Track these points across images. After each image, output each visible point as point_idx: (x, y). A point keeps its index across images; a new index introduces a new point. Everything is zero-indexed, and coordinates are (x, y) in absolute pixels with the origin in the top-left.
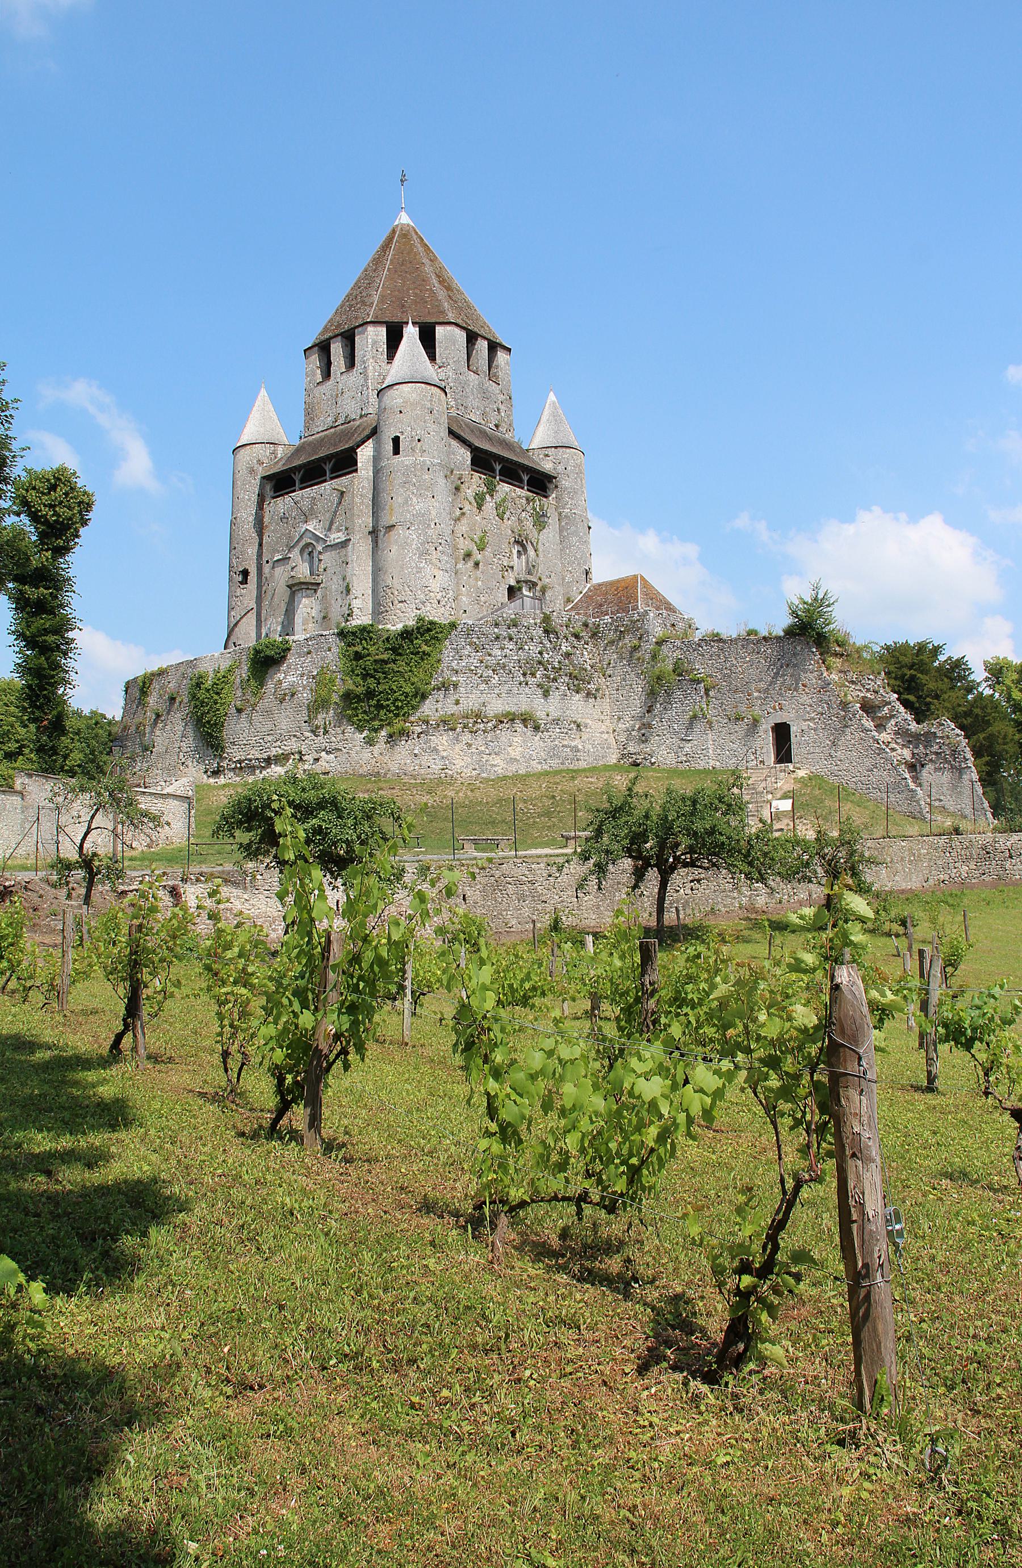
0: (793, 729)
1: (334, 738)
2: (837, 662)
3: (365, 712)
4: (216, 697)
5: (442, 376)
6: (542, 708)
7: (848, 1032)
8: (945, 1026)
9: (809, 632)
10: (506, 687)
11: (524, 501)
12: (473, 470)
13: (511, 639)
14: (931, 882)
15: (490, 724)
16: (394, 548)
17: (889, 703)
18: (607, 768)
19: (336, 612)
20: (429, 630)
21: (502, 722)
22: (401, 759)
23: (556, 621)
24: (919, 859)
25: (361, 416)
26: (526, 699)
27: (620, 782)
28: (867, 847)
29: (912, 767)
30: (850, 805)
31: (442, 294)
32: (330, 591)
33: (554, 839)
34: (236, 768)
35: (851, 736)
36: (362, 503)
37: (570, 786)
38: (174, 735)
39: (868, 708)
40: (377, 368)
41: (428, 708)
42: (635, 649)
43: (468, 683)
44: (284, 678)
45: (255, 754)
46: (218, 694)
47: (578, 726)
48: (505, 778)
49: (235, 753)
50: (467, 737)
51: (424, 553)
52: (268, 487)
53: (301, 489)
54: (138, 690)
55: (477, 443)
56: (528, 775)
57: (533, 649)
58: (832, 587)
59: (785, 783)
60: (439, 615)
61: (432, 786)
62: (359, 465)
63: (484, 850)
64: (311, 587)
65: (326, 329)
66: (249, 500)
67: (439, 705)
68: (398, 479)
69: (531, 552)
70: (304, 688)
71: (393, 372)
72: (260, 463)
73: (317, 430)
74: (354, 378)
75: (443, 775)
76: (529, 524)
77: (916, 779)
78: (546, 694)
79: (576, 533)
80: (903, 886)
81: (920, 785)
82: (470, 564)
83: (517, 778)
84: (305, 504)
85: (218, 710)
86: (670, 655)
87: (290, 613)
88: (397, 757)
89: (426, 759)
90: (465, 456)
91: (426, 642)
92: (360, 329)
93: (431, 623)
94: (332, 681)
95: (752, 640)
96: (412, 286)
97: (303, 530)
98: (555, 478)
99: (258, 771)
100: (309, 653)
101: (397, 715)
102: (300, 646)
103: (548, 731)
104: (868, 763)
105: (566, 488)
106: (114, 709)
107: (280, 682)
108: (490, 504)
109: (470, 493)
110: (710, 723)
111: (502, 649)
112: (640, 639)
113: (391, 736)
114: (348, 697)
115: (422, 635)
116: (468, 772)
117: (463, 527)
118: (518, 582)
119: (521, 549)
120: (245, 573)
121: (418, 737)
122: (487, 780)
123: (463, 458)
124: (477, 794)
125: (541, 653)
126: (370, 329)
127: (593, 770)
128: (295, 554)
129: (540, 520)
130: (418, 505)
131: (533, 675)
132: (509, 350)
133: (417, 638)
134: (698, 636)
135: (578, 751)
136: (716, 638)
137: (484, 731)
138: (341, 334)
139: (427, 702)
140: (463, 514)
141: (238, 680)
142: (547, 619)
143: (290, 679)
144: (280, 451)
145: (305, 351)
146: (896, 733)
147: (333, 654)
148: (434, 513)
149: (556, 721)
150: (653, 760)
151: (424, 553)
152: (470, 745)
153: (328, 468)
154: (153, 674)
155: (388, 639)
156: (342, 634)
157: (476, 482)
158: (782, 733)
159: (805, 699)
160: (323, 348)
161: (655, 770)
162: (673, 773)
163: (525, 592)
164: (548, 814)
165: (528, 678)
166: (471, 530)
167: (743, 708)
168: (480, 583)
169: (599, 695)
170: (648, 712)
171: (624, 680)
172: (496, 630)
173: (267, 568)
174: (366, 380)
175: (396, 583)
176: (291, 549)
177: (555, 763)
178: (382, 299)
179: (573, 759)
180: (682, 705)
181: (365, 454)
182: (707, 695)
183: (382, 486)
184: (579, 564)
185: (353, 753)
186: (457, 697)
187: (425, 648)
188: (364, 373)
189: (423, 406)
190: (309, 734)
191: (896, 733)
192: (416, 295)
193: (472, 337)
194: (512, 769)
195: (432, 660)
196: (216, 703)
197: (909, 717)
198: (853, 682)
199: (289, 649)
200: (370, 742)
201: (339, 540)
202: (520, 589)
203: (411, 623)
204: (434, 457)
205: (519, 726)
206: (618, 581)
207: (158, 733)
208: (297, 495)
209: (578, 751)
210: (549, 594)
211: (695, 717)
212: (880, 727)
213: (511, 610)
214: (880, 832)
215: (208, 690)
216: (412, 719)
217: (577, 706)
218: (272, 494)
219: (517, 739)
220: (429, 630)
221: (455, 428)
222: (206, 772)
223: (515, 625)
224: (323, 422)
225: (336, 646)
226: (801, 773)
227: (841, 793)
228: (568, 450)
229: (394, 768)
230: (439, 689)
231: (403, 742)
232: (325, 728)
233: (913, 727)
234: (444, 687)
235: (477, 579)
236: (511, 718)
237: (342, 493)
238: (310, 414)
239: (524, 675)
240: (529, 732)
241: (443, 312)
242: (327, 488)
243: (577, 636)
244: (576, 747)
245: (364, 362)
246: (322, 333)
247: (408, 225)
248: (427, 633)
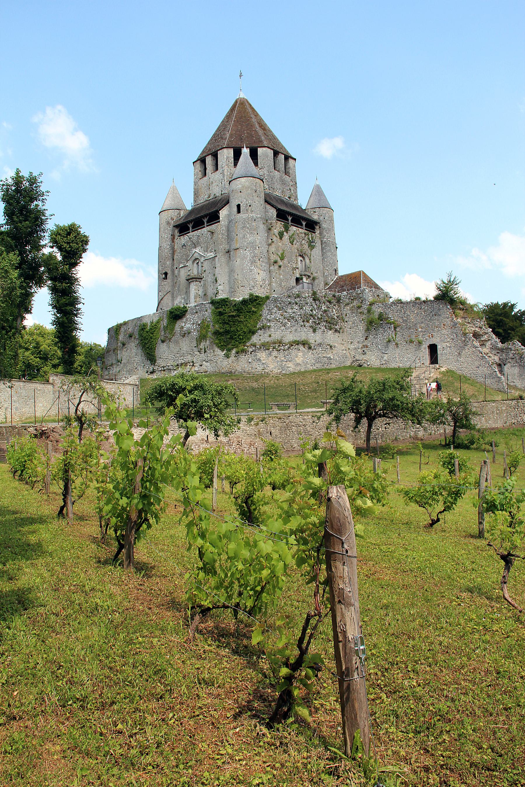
0: (439, 347)
1: (210, 355)
2: (461, 313)
3: (224, 341)
4: (151, 335)
5: (261, 173)
6: (314, 338)
7: (335, 527)
8: (487, 503)
9: (446, 297)
10: (294, 328)
11: (303, 235)
12: (277, 220)
13: (297, 304)
14: (508, 424)
15: (286, 347)
16: (238, 260)
17: (487, 333)
18: (345, 367)
19: (211, 292)
20: (256, 300)
21: (292, 345)
22: (242, 364)
23: (319, 295)
24: (501, 412)
25: (222, 194)
26: (305, 333)
27: (351, 374)
28: (474, 406)
29: (499, 365)
30: (467, 385)
31: (261, 132)
32: (208, 282)
33: (318, 403)
34: (162, 370)
35: (468, 351)
36: (222, 238)
37: (326, 377)
38: (132, 353)
39: (476, 335)
40: (229, 170)
41: (255, 339)
42: (359, 307)
43: (275, 327)
44: (185, 325)
45: (170, 363)
46: (152, 334)
48: (294, 373)
49: (160, 362)
50: (275, 353)
51: (253, 262)
52: (176, 231)
53: (192, 231)
54: (114, 332)
55: (280, 207)
56: (306, 372)
57: (307, 309)
58: (458, 275)
59: (434, 375)
60: (260, 293)
61: (257, 377)
62: (221, 219)
63: (282, 410)
64: (198, 279)
65: (203, 152)
66: (167, 238)
67: (261, 338)
68: (240, 226)
69: (307, 261)
70: (194, 330)
71: (237, 171)
72: (172, 219)
73: (200, 202)
74: (217, 176)
75: (263, 372)
76: (306, 246)
77: (501, 372)
78: (314, 331)
79: (330, 251)
80: (494, 426)
81: (504, 375)
82: (276, 267)
83: (300, 373)
84: (195, 239)
85: (153, 342)
86: (377, 310)
87: (187, 293)
88: (240, 363)
89: (255, 365)
90: (273, 212)
91: (254, 306)
92: (220, 151)
93: (257, 297)
94: (208, 326)
95: (417, 302)
96: (246, 129)
97: (193, 252)
98: (319, 223)
99: (172, 372)
100: (197, 313)
101: (240, 343)
102: (192, 309)
103: (315, 350)
104: (477, 363)
105: (325, 228)
106: (102, 341)
107: (182, 327)
108: (286, 236)
109: (276, 232)
110: (397, 344)
112: (361, 303)
113: (237, 353)
114: (216, 333)
115: (252, 302)
116: (276, 371)
117: (273, 249)
118: (301, 275)
119: (302, 259)
120: (166, 274)
121: (251, 354)
122: (285, 374)
123: (272, 214)
124: (280, 381)
125: (311, 311)
126: (225, 150)
127: (338, 369)
128: (190, 263)
129: (311, 246)
131: (308, 321)
132: (295, 159)
133: (249, 304)
134: (391, 300)
135: (331, 359)
136: (399, 302)
137: (284, 350)
138: (211, 154)
139: (255, 336)
140: (273, 242)
141: (162, 327)
142: (314, 293)
143: (187, 326)
144: (182, 213)
145: (193, 163)
146: (491, 348)
147: (208, 313)
148: (258, 242)
149: (320, 345)
150: (368, 364)
151: (253, 262)
152: (277, 357)
153: (205, 221)
154: (121, 325)
155: (235, 305)
156: (213, 303)
157: (279, 226)
158: (433, 348)
159: (444, 331)
160: (202, 160)
161: (369, 368)
162: (379, 370)
163: (304, 280)
164: (315, 391)
165: (305, 323)
166: (277, 250)
167: (413, 337)
168: (281, 276)
169: (341, 331)
170: (366, 339)
171: (354, 323)
173: (176, 272)
174: (224, 176)
175: (240, 277)
176: (187, 261)
177: (319, 366)
178: (231, 136)
179: (328, 364)
180: (382, 335)
181: (223, 213)
182: (395, 330)
183: (231, 229)
184: (331, 266)
185: (219, 362)
186: (269, 333)
187: (253, 309)
188: (223, 173)
189: (252, 189)
190: (196, 353)
191: (491, 348)
192: (248, 133)
193: (276, 153)
194: (298, 368)
195: (258, 315)
196: (151, 338)
197: (498, 340)
198: (469, 323)
199: (187, 311)
200: (227, 356)
201: (211, 257)
202: (302, 279)
203: (247, 297)
204: (258, 214)
205: (301, 347)
206: (351, 274)
207: (124, 353)
208: (191, 234)
209: (331, 359)
210: (317, 281)
211: (389, 341)
212: (483, 345)
213: (296, 291)
214: (481, 398)
215: (147, 332)
216: (248, 344)
217: (330, 337)
218: (178, 234)
219: (300, 354)
220: (256, 300)
221: (268, 199)
222: (147, 372)
224: (203, 199)
225: (210, 308)
226: (443, 369)
227: (461, 378)
229: (239, 369)
230: (261, 329)
231: (243, 356)
232: (205, 350)
233: (500, 345)
234: (263, 328)
235: (280, 275)
236: (297, 343)
237: (213, 233)
238: (196, 194)
239: (303, 321)
240: (306, 350)
241: (261, 141)
242: (205, 231)
243: (330, 302)
244: (330, 357)
245: (223, 168)
246: (202, 154)
247: (244, 98)
248: (254, 302)
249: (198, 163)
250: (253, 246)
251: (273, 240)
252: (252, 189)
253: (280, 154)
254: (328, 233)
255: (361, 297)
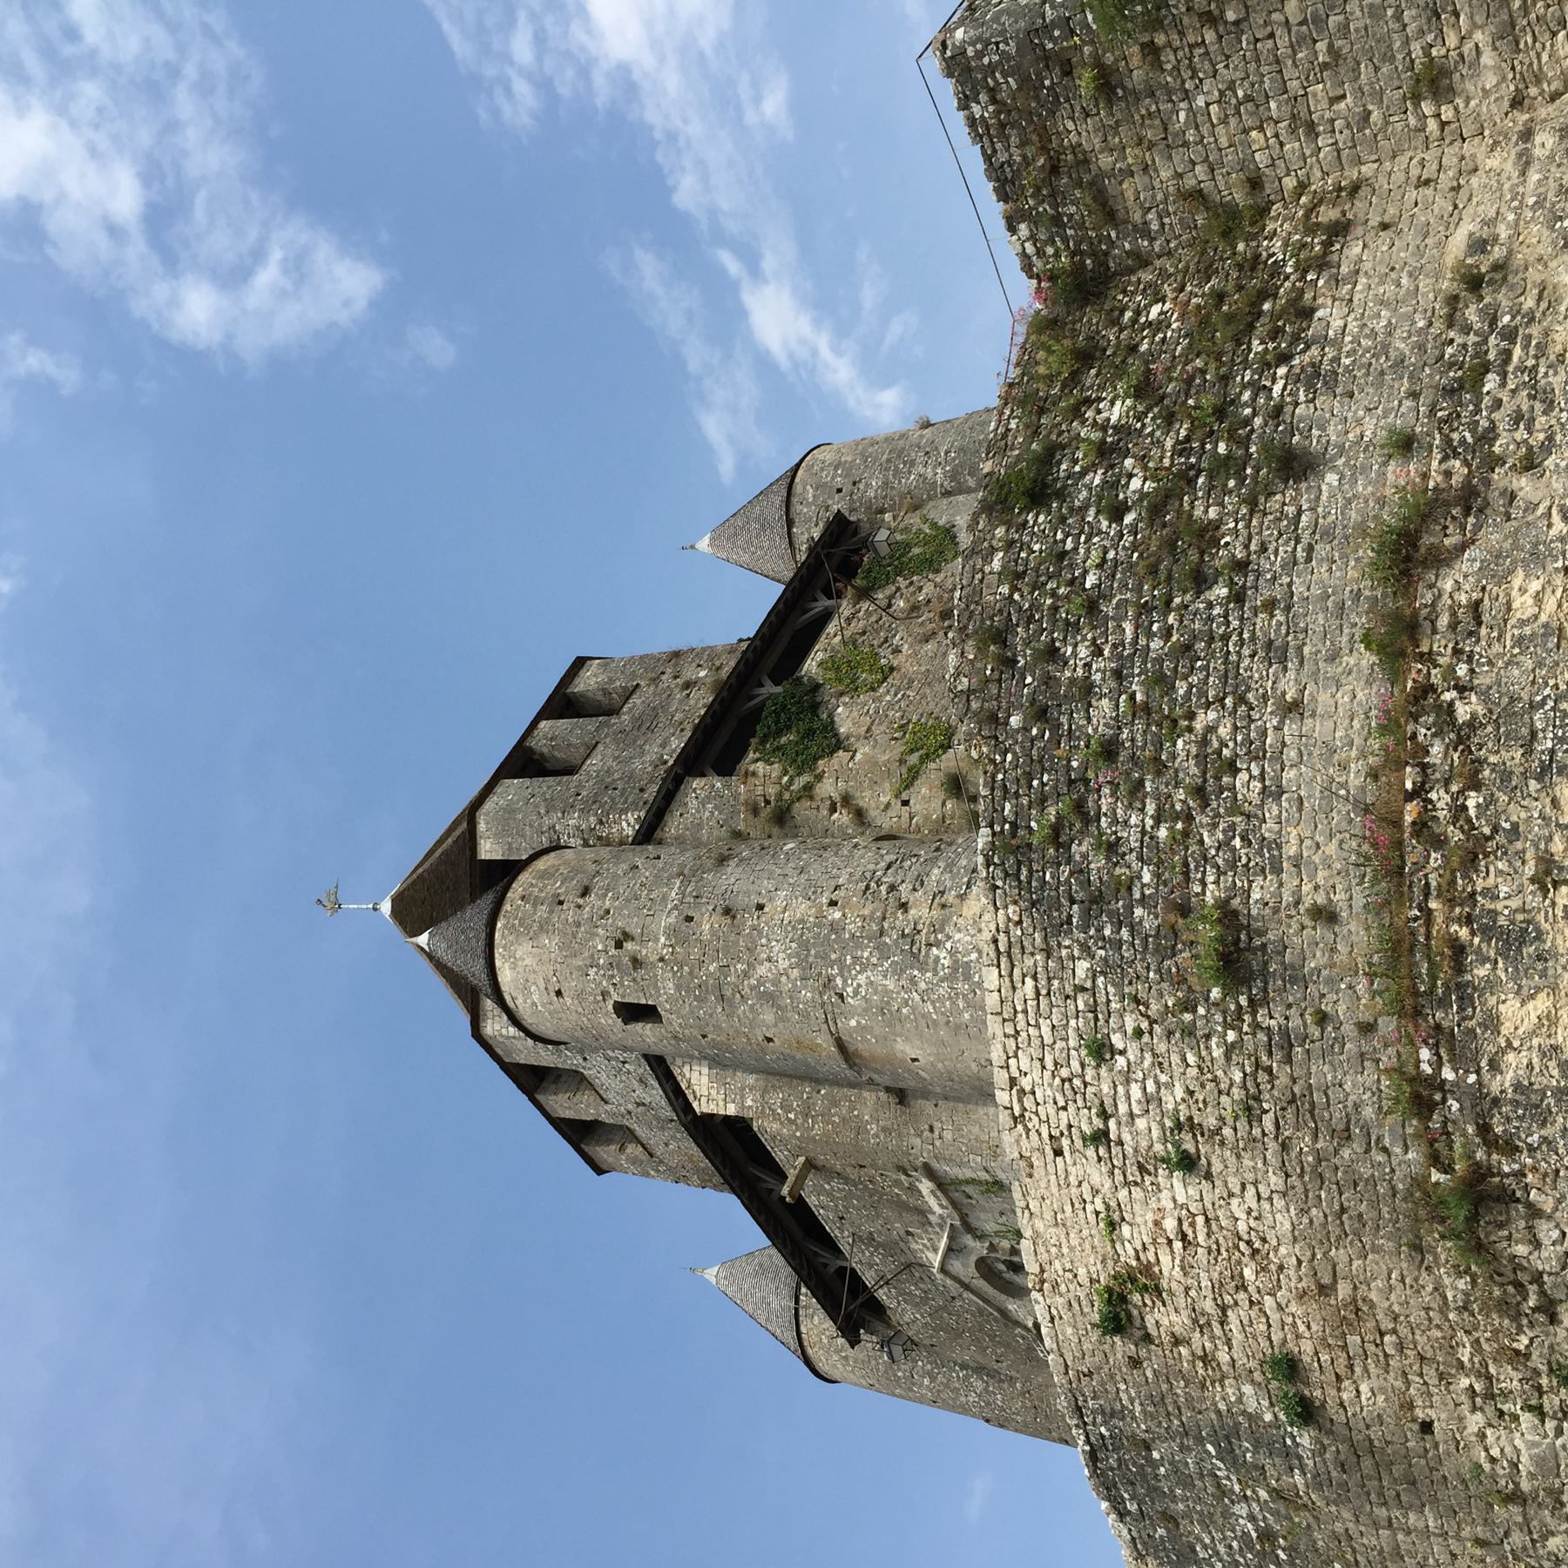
10: (1253, 669)
16: (906, 1048)
47: (1474, 283)
50: (1504, 886)
62: (732, 1110)
66: (933, 1379)
103: (1489, 436)
111: (1087, 690)
121: (1509, 1148)
130: (777, 960)
131: (1208, 535)
140: (846, 800)
145: (599, 1171)
148: (802, 908)
172: (1015, 721)
181: (709, 1093)
204: (664, 899)
223: (1000, 637)
228: (798, 488)
236: (1398, 639)
239: (1200, 582)
249: (605, 1153)
250: (819, 949)
251: (836, 796)
252: (545, 927)
253: (531, 743)
254: (913, 463)
255: (1024, 81)
